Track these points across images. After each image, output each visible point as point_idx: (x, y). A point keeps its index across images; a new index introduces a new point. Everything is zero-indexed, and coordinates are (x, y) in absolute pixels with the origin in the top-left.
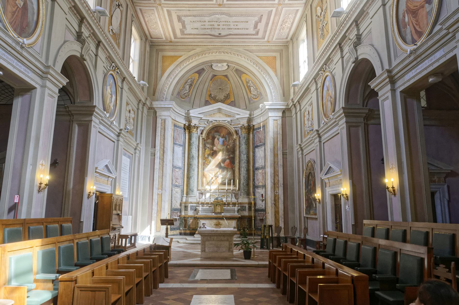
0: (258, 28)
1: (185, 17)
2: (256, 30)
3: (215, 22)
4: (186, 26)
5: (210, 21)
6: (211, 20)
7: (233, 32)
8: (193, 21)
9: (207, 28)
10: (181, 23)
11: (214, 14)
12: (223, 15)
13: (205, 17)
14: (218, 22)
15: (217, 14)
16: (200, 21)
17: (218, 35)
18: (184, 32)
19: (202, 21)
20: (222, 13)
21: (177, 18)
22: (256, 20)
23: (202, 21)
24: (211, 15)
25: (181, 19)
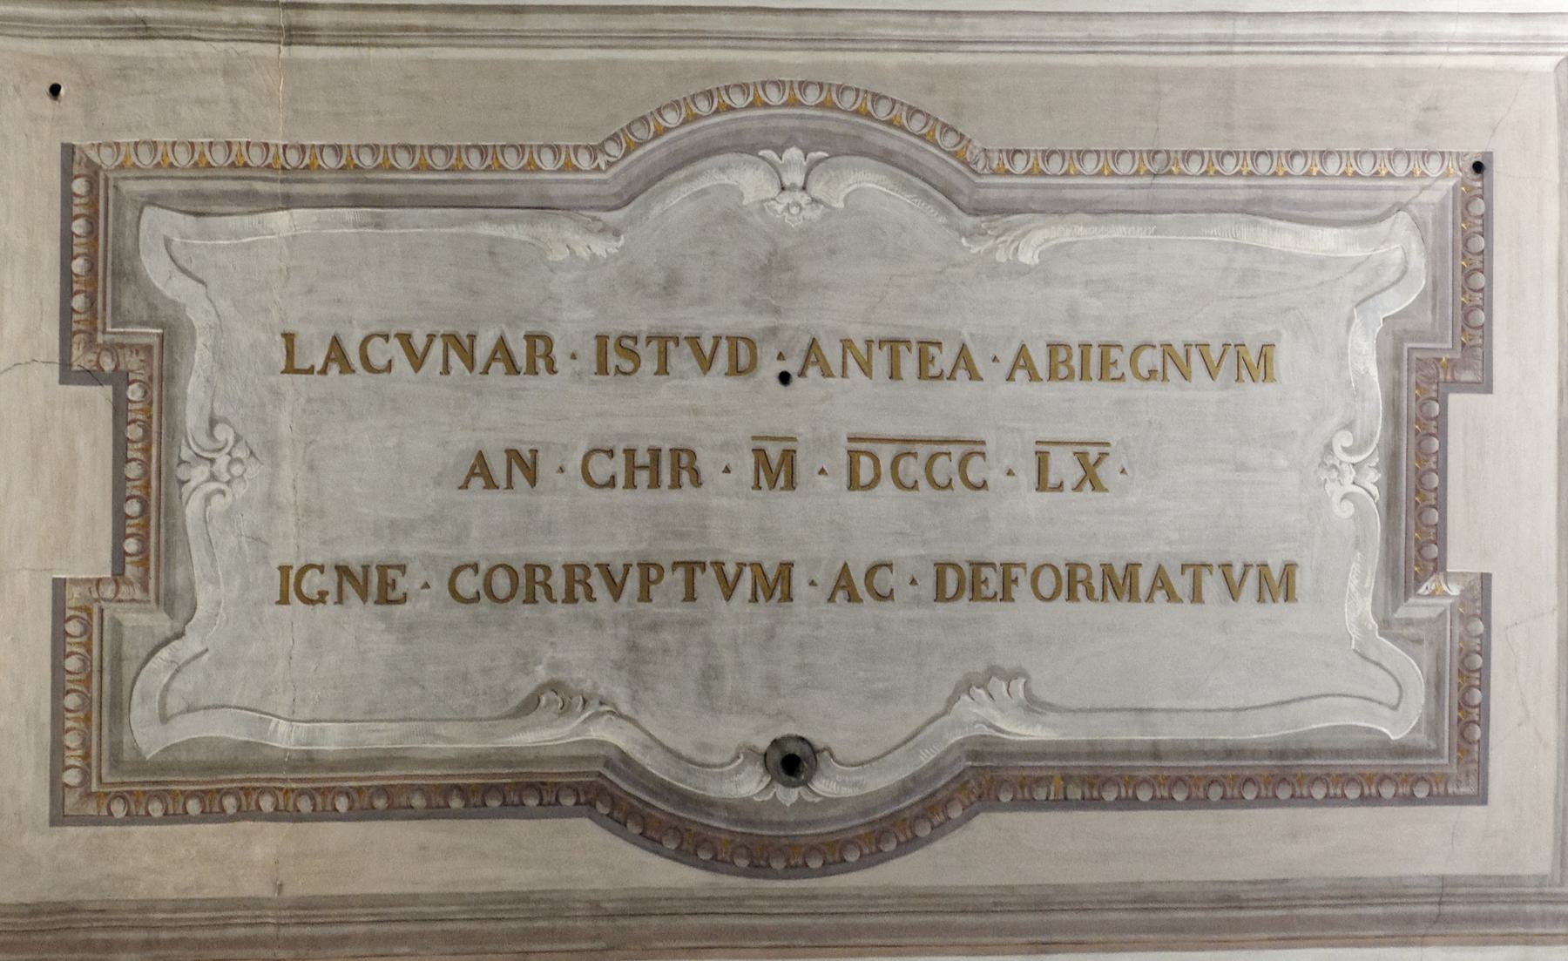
0: (1461, 558)
1: (199, 206)
2: (1419, 608)
3: (716, 382)
4: (192, 510)
5: (627, 346)
6: (643, 320)
7: (1033, 706)
8: (337, 350)
9: (558, 551)
10: (101, 395)
11: (713, 125)
12: (859, 149)
13: (544, 207)
14: (770, 368)
15: (746, 146)
16: (452, 340)
17: (750, 785)
18: (119, 708)
19: (484, 347)
20: (832, 93)
21: (50, 250)
22: (1395, 302)
23: (484, 347)
24: (654, 151)
25: (125, 272)
